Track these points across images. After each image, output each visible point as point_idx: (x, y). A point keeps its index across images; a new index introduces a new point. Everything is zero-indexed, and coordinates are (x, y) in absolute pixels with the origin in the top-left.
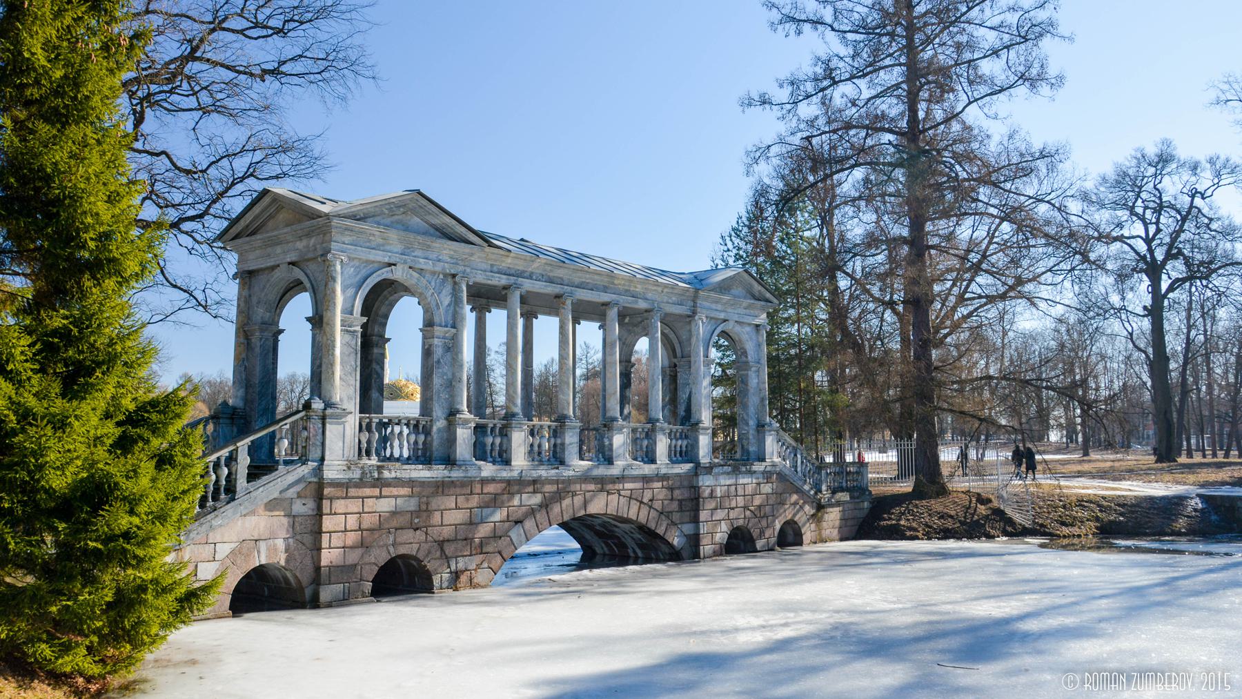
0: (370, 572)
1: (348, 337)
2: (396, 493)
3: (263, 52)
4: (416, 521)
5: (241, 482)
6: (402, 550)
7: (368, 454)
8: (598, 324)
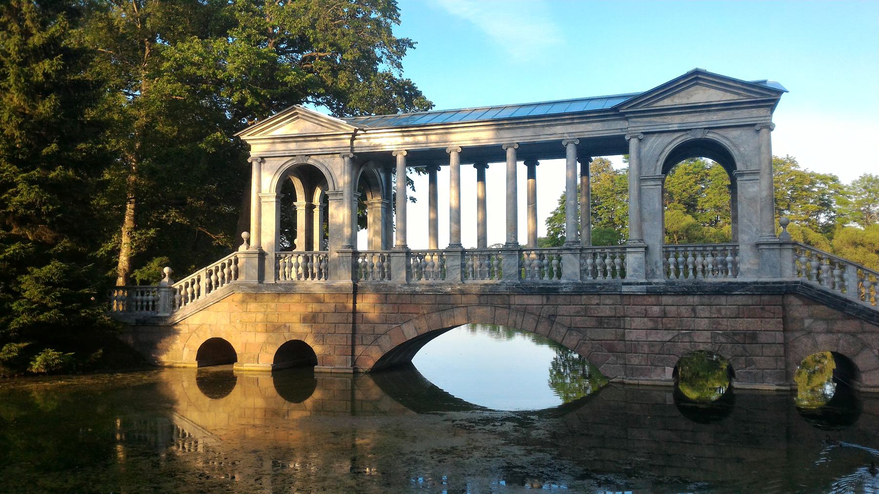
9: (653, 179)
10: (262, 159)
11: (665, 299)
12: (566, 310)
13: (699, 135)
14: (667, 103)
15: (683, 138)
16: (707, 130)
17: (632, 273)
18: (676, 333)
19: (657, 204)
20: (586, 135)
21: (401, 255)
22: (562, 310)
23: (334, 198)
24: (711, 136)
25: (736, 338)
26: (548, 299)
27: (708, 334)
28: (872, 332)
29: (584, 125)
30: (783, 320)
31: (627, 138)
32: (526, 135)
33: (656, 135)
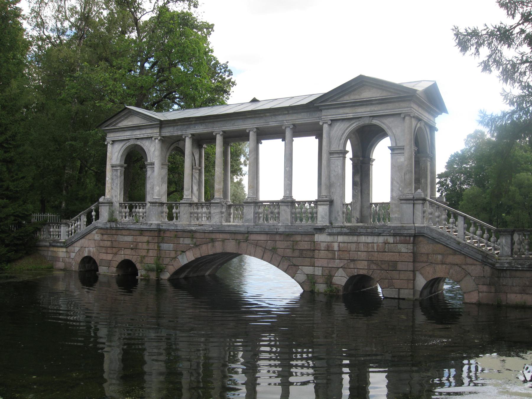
0: (116, 264)
1: (115, 173)
2: (124, 234)
4: (132, 246)
6: (127, 257)
7: (125, 217)
9: (338, 153)
10: (114, 142)
12: (281, 245)
13: (367, 121)
14: (347, 99)
15: (357, 123)
16: (371, 118)
17: (320, 219)
19: (340, 170)
20: (298, 122)
22: (280, 245)
24: (375, 122)
25: (383, 266)
27: (366, 263)
28: (472, 265)
29: (296, 115)
30: (413, 255)
31: (321, 123)
32: (260, 123)
33: (340, 121)
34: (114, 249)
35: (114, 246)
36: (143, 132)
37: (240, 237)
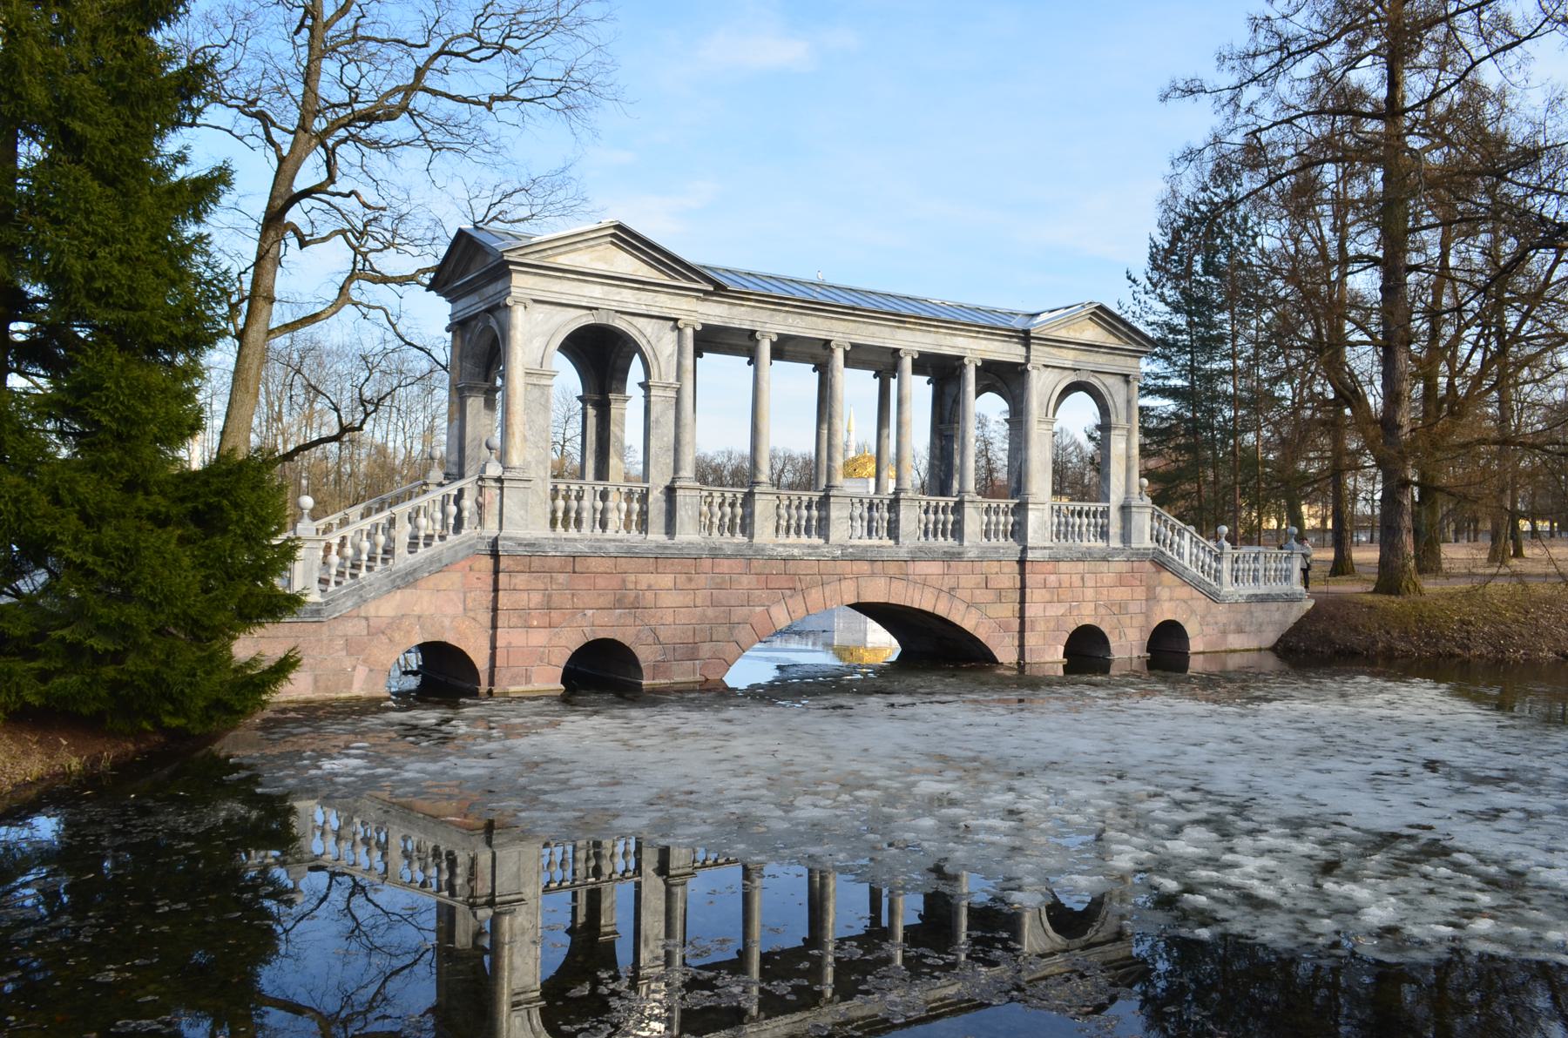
0: (561, 658)
1: (536, 393)
3: (490, 77)
5: (401, 548)
6: (601, 635)
7: (566, 526)
8: (927, 378)
11: (1063, 566)
13: (1083, 377)
18: (1067, 605)
21: (770, 497)
23: (661, 393)
24: (1093, 380)
26: (949, 566)
31: (1029, 367)
34: (554, 614)
35: (553, 606)
36: (646, 297)
37: (892, 569)
